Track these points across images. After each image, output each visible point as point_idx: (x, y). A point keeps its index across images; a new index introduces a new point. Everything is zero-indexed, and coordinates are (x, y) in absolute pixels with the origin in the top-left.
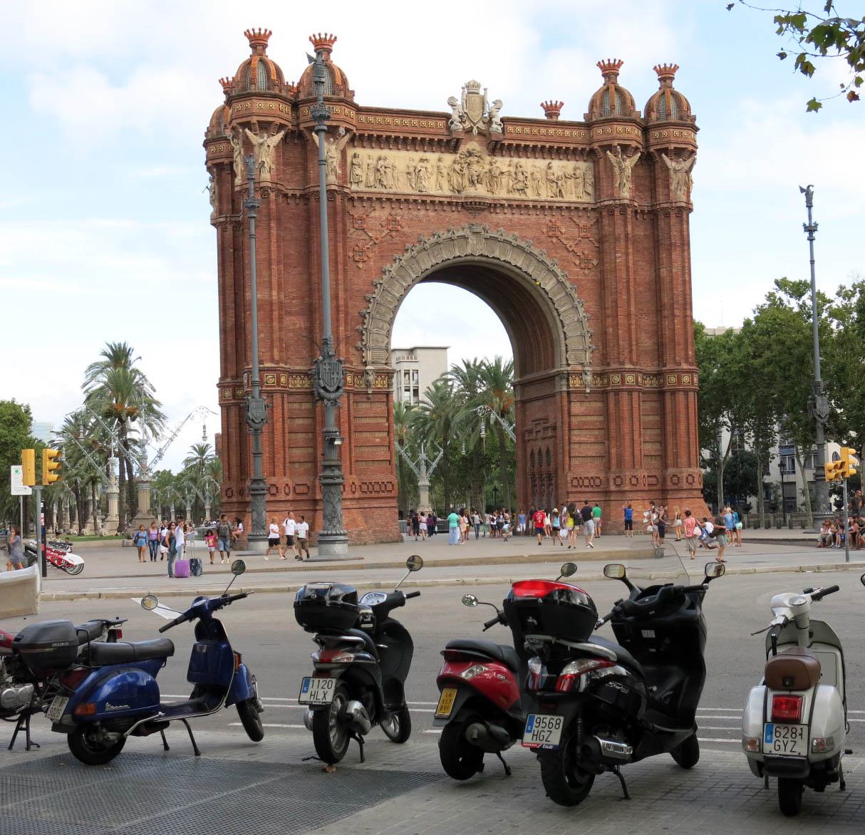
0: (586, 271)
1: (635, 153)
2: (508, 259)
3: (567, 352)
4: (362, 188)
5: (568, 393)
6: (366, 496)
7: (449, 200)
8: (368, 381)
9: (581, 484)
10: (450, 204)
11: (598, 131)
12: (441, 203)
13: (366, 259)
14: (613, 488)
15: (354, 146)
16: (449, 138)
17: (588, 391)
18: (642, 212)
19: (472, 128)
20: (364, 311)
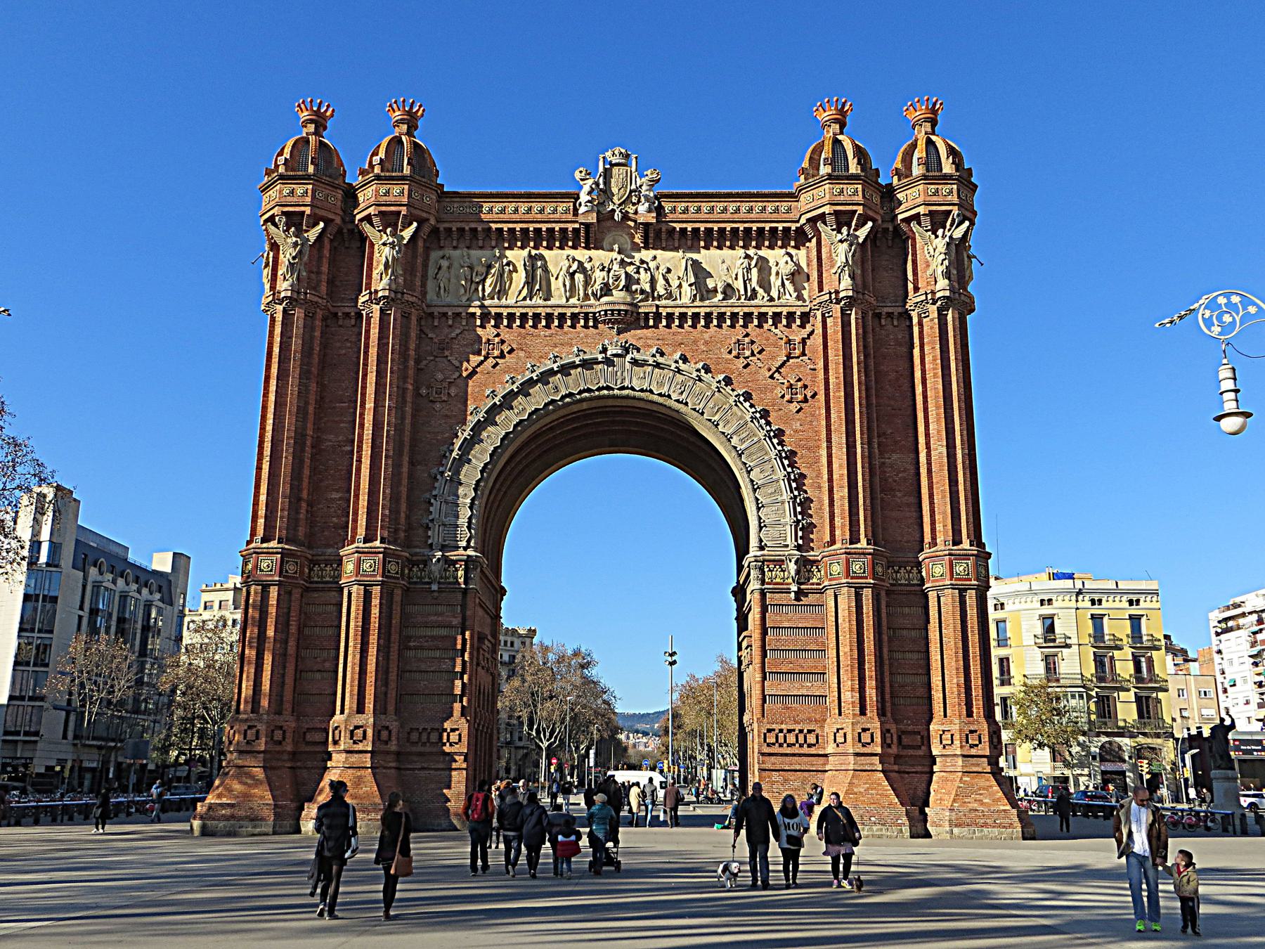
0: (794, 407)
1: (864, 224)
2: (664, 390)
3: (761, 528)
4: (449, 300)
5: (763, 594)
6: (414, 749)
7: (576, 311)
8: (430, 572)
9: (781, 740)
13: (445, 398)
14: (830, 749)
15: (441, 248)
16: (577, 226)
17: (794, 588)
18: (890, 315)
19: (613, 211)
20: (434, 471)
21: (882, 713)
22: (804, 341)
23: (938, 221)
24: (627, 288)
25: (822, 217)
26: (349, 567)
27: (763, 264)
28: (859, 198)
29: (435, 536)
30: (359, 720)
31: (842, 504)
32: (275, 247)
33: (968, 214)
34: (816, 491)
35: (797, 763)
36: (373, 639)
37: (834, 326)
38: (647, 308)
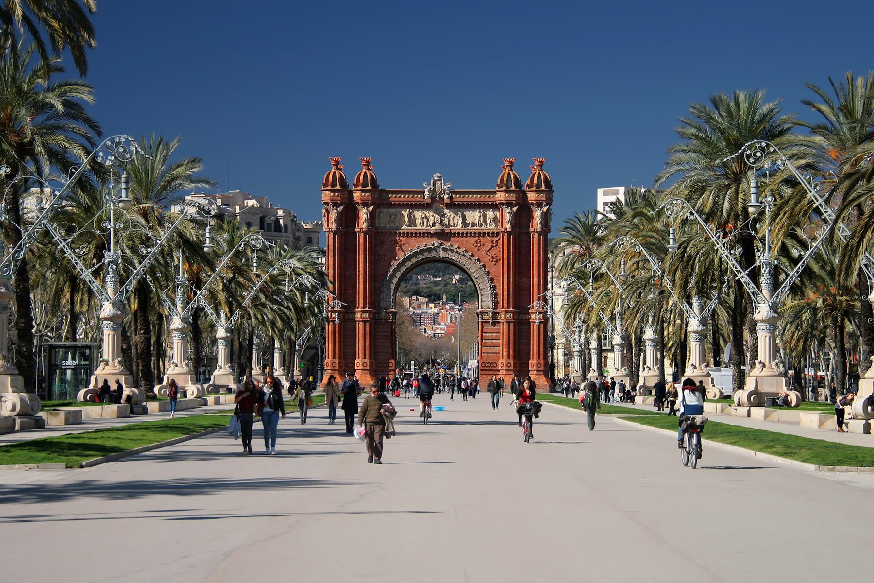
10: (424, 233)
11: (498, 195)
12: (420, 233)
21: (514, 358)
22: (497, 241)
23: (539, 205)
24: (441, 223)
25: (502, 204)
26: (358, 316)
27: (485, 216)
28: (514, 198)
29: (383, 304)
30: (365, 360)
31: (505, 297)
32: (328, 212)
33: (549, 202)
34: (499, 291)
35: (491, 372)
36: (367, 337)
37: (506, 240)
38: (447, 230)
